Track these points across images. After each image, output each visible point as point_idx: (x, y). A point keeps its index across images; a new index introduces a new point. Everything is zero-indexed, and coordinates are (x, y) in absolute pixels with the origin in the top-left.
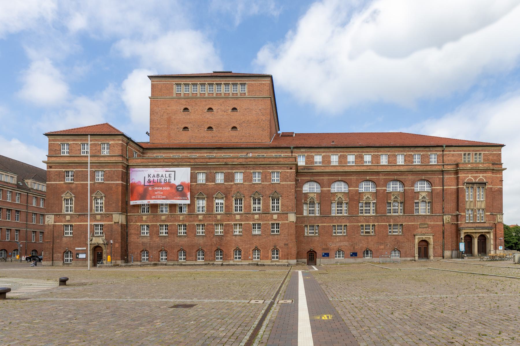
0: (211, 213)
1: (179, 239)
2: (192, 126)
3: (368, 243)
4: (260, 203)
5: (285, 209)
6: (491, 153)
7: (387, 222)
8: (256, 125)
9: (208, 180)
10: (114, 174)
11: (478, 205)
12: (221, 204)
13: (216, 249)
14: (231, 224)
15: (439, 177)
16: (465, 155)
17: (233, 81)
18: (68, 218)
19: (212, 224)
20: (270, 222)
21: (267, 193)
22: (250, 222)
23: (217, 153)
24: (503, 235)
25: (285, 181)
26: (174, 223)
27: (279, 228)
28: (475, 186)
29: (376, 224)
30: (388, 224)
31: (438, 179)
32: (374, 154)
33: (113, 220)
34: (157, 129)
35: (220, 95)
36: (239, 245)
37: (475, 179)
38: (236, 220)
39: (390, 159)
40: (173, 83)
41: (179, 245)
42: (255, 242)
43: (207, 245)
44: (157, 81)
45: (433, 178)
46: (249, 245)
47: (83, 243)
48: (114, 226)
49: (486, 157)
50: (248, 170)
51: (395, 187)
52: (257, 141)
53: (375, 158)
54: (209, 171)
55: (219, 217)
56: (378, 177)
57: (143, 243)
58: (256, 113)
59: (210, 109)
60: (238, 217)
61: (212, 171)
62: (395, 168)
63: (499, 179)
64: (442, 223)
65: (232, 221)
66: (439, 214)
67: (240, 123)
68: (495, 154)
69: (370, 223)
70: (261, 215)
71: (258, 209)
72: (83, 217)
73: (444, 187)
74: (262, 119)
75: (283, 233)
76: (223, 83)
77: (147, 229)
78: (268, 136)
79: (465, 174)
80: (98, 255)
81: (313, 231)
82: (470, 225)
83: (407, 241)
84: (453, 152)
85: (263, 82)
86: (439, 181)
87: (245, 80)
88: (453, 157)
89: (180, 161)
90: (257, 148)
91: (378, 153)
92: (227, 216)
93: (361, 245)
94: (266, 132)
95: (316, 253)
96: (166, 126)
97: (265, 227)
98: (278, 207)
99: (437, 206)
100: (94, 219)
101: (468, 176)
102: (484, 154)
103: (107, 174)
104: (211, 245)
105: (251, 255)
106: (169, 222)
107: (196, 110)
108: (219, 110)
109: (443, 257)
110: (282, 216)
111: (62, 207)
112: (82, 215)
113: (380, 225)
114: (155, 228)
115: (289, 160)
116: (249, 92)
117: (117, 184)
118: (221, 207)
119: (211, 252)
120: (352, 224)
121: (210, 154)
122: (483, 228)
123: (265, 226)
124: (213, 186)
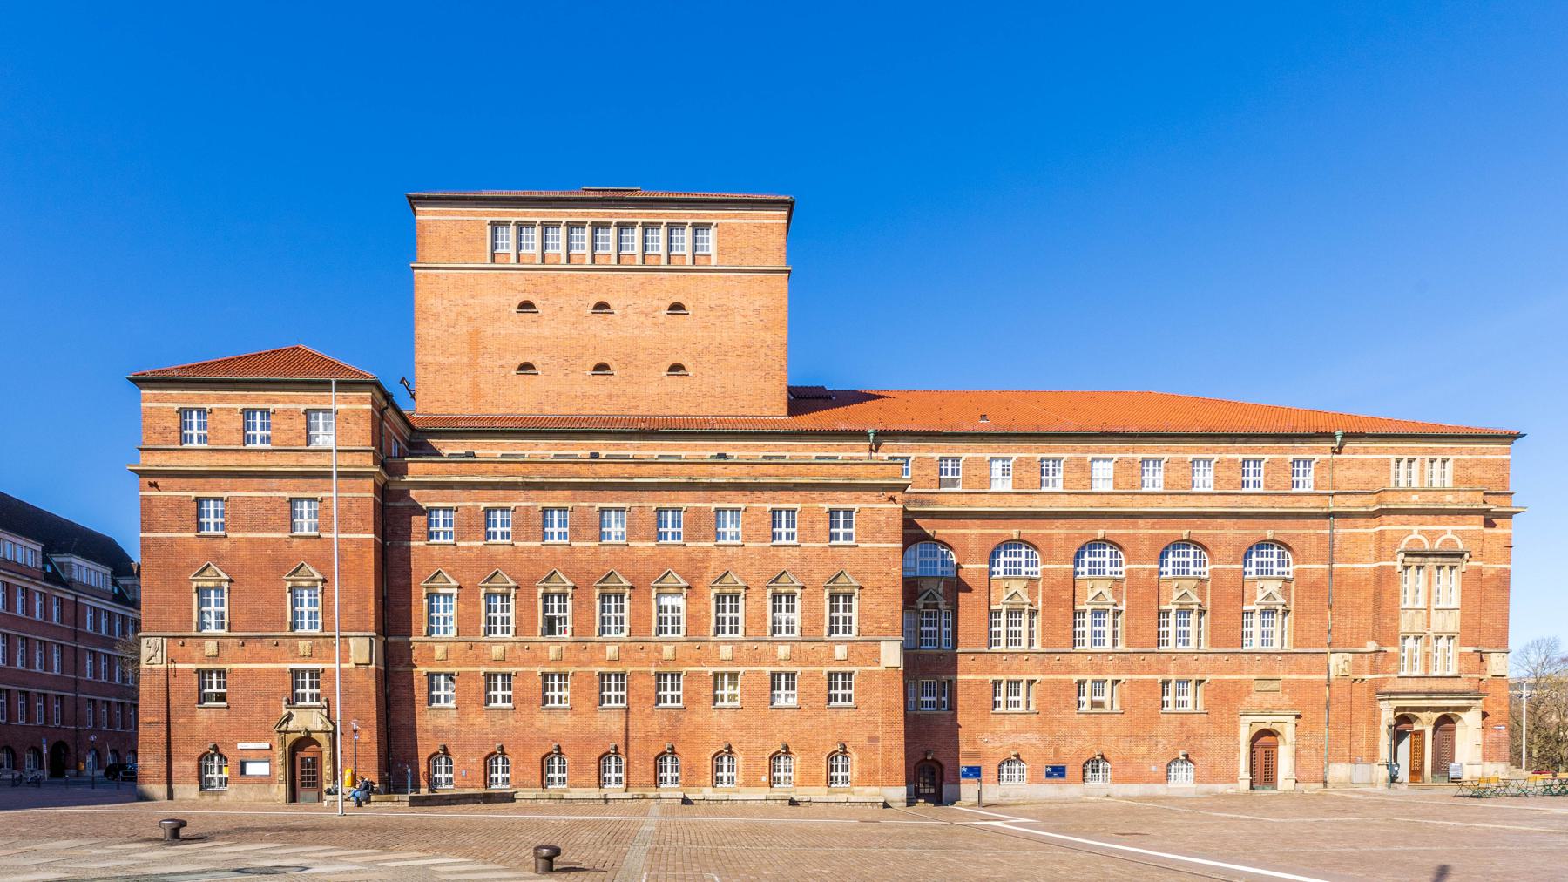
0: (644, 638)
1: (546, 720)
2: (547, 361)
3: (1098, 735)
4: (793, 607)
5: (870, 628)
6: (1479, 460)
7: (1160, 672)
8: (744, 359)
9: (634, 533)
10: (350, 509)
11: (1439, 623)
12: (673, 611)
14: (707, 672)
15: (1319, 531)
16: (1398, 461)
17: (672, 217)
20: (826, 670)
21: (817, 576)
22: (762, 669)
23: (638, 449)
24: (1505, 716)
25: (873, 540)
26: (532, 669)
27: (850, 688)
28: (1431, 562)
31: (1315, 540)
32: (1121, 459)
33: (350, 656)
34: (437, 368)
35: (630, 262)
36: (731, 738)
37: (1432, 541)
38: (722, 662)
39: (1173, 475)
40: (486, 218)
42: (781, 732)
45: (1298, 535)
46: (761, 741)
47: (261, 729)
48: (354, 674)
49: (1462, 473)
50: (758, 502)
51: (1099, 563)
52: (746, 411)
53: (1126, 469)
54: (637, 504)
56: (1132, 531)
57: (437, 731)
58: (745, 320)
59: (601, 306)
60: (726, 651)
61: (646, 504)
62: (1186, 504)
63: (1503, 542)
64: (1326, 677)
65: (708, 662)
66: (1315, 650)
67: (695, 354)
68: (1490, 463)
69: (1108, 674)
70: (797, 644)
71: (787, 628)
72: (258, 645)
73: (1334, 566)
74: (763, 341)
75: (863, 703)
76: (640, 224)
77: (446, 687)
78: (781, 394)
79: (1402, 524)
80: (303, 766)
81: (932, 699)
82: (1412, 685)
83: (1217, 730)
84: (1365, 453)
85: (766, 221)
86: (1319, 545)
87: (711, 215)
88: (1362, 468)
89: (547, 472)
90: (763, 433)
91: (1135, 456)
92: (694, 648)
94: (776, 382)
95: (941, 766)
97: (811, 684)
98: (850, 622)
99: (1311, 625)
100: (291, 651)
101: (1411, 532)
102: (1458, 460)
105: (767, 772)
106: (516, 665)
107: (557, 308)
108: (630, 311)
109: (1325, 783)
110: (862, 648)
111: (192, 613)
113: (1138, 680)
116: (721, 251)
117: (361, 543)
118: (616, 618)
120: (1052, 677)
121: (617, 450)
122: (1452, 694)
123: (809, 679)
124: (649, 552)
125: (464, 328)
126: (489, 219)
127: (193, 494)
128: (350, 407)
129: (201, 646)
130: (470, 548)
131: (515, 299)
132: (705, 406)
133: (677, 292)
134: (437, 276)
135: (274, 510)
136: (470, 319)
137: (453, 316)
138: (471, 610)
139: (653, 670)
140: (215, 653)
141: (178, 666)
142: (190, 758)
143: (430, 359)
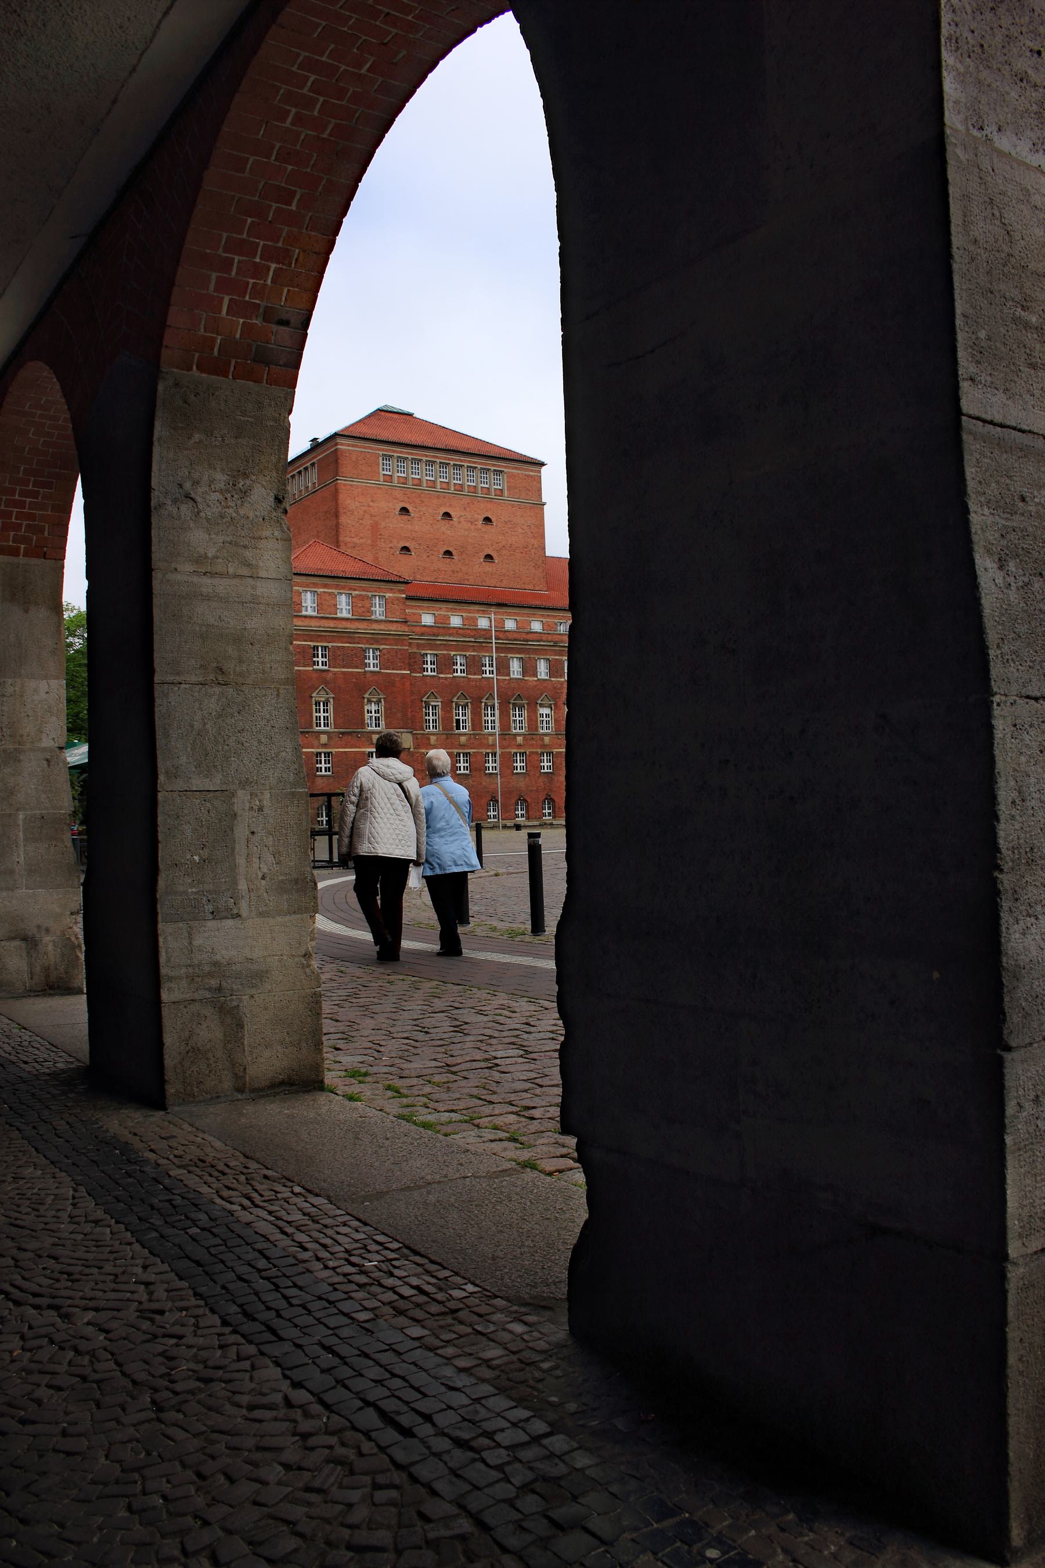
13: (545, 797)
19: (537, 753)
41: (488, 792)
44: (349, 445)
55: (547, 739)
61: (532, 656)
74: (533, 545)
96: (369, 542)
104: (537, 791)
108: (462, 519)
112: (348, 733)
119: (538, 803)
124: (535, 683)
125: (367, 521)
126: (381, 453)
127: (312, 644)
128: (396, 595)
129: (318, 738)
130: (446, 678)
132: (505, 582)
133: (487, 511)
134: (351, 485)
136: (371, 516)
137: (361, 512)
138: (447, 715)
139: (539, 751)
143: (348, 539)
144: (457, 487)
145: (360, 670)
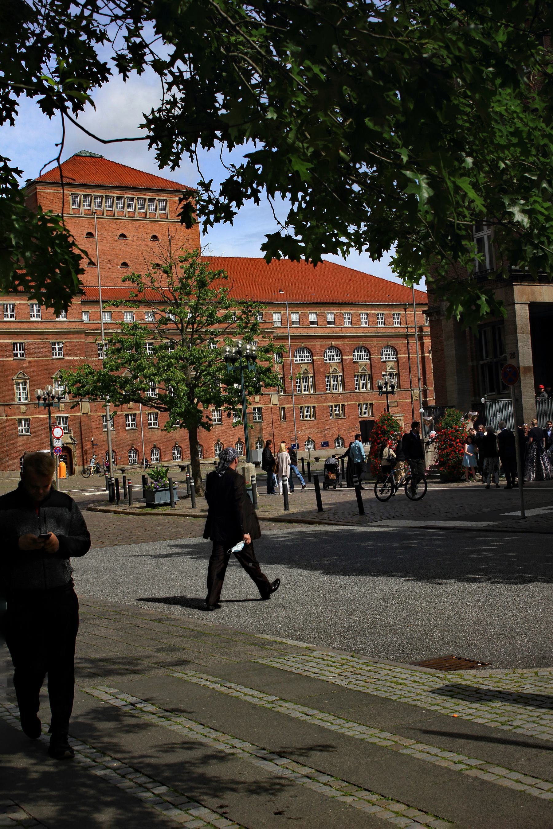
10: (76, 346)
18: (23, 408)
29: (345, 403)
30: (357, 403)
31: (403, 345)
43: (184, 439)
93: (332, 431)
103: (66, 346)
108: (135, 238)
114: (120, 419)
115: (265, 327)
127: (12, 341)
129: (19, 409)
131: (84, 231)
135: (45, 347)
140: (25, 411)
141: (9, 418)
142: (16, 459)
144: (131, 214)
145: (48, 358)
